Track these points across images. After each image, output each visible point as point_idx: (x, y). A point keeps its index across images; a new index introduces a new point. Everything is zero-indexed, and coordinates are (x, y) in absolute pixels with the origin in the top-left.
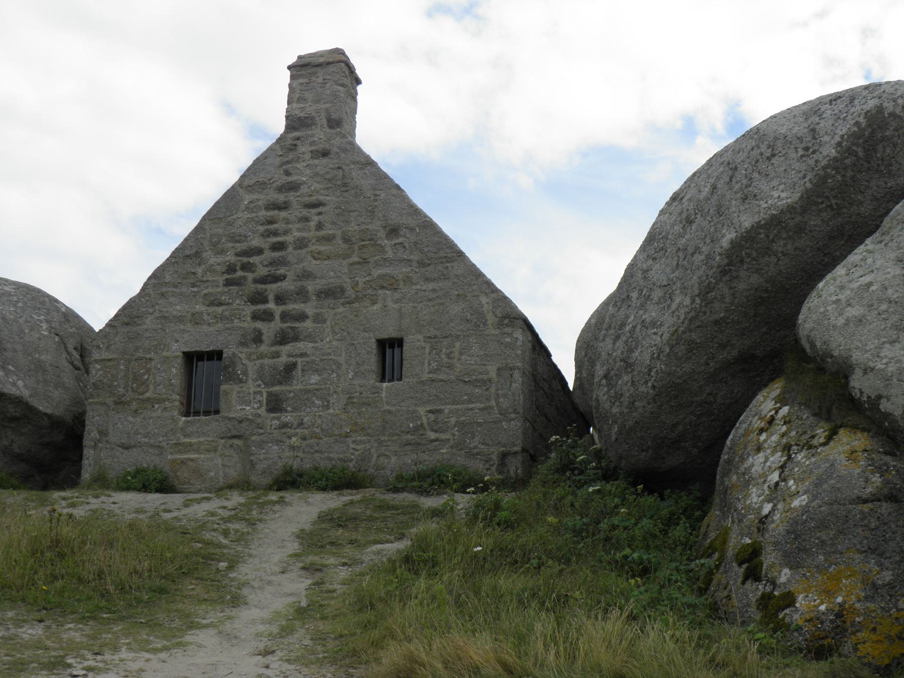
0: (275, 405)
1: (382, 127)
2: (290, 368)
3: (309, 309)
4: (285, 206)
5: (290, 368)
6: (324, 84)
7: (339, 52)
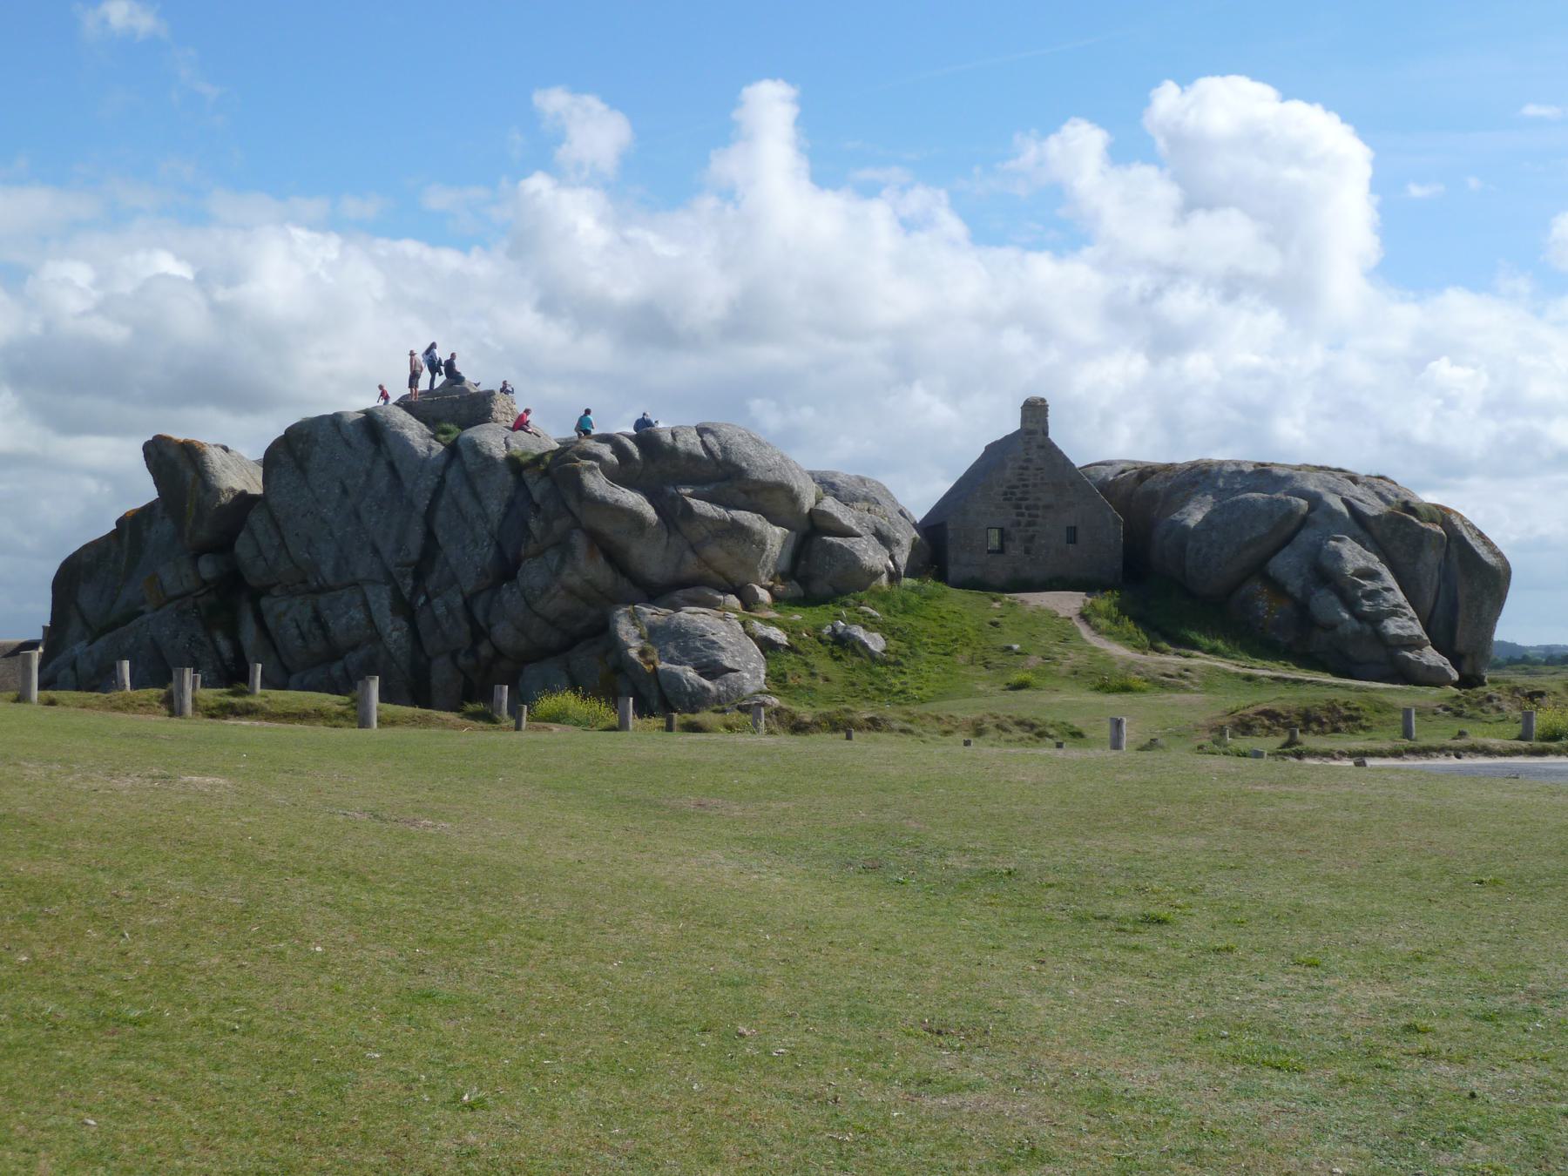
0: (1027, 551)
1: (1061, 434)
2: (1033, 537)
3: (1039, 513)
4: (1026, 468)
5: (1033, 537)
6: (1035, 411)
7: (1043, 400)
